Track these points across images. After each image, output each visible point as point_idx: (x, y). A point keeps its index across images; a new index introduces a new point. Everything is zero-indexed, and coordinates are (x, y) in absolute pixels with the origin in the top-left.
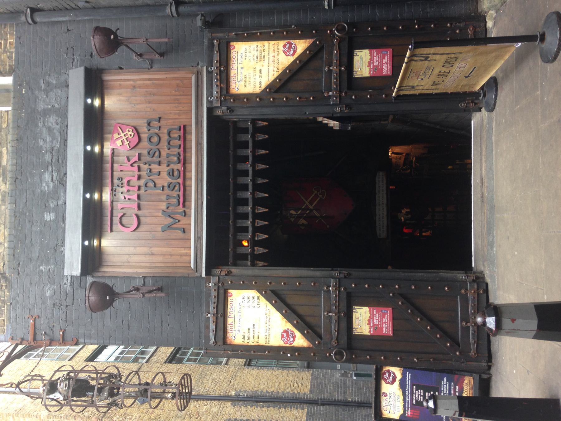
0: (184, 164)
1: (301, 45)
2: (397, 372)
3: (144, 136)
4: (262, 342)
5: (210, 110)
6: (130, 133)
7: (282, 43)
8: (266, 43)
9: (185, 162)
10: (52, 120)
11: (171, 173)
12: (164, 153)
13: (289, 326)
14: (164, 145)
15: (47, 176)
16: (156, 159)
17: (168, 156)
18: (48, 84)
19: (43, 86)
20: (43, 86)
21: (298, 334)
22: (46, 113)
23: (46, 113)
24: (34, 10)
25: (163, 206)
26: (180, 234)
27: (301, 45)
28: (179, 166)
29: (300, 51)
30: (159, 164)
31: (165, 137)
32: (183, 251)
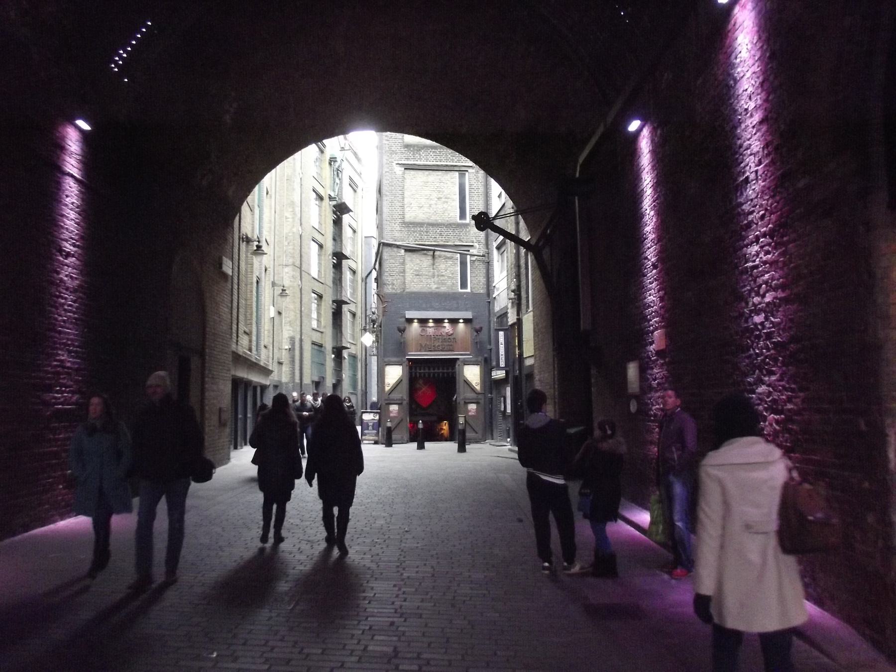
0: (441, 350)
1: (478, 388)
2: (377, 417)
3: (450, 337)
4: (386, 377)
5: (458, 359)
6: (451, 332)
7: (479, 381)
8: (479, 377)
9: (442, 351)
10: (455, 306)
11: (439, 346)
12: (445, 343)
13: (391, 385)
14: (448, 344)
15: (437, 304)
16: (443, 341)
17: (444, 345)
18: (467, 304)
19: (466, 302)
20: (466, 302)
21: (389, 388)
22: (458, 303)
23: (458, 303)
24: (489, 302)
25: (428, 343)
26: (419, 349)
27: (478, 388)
28: (441, 349)
29: (476, 387)
30: (442, 342)
31: (450, 344)
32: (414, 350)
